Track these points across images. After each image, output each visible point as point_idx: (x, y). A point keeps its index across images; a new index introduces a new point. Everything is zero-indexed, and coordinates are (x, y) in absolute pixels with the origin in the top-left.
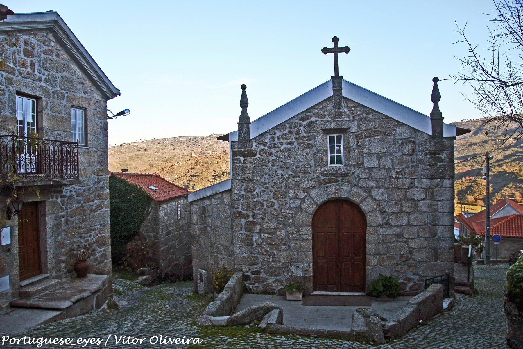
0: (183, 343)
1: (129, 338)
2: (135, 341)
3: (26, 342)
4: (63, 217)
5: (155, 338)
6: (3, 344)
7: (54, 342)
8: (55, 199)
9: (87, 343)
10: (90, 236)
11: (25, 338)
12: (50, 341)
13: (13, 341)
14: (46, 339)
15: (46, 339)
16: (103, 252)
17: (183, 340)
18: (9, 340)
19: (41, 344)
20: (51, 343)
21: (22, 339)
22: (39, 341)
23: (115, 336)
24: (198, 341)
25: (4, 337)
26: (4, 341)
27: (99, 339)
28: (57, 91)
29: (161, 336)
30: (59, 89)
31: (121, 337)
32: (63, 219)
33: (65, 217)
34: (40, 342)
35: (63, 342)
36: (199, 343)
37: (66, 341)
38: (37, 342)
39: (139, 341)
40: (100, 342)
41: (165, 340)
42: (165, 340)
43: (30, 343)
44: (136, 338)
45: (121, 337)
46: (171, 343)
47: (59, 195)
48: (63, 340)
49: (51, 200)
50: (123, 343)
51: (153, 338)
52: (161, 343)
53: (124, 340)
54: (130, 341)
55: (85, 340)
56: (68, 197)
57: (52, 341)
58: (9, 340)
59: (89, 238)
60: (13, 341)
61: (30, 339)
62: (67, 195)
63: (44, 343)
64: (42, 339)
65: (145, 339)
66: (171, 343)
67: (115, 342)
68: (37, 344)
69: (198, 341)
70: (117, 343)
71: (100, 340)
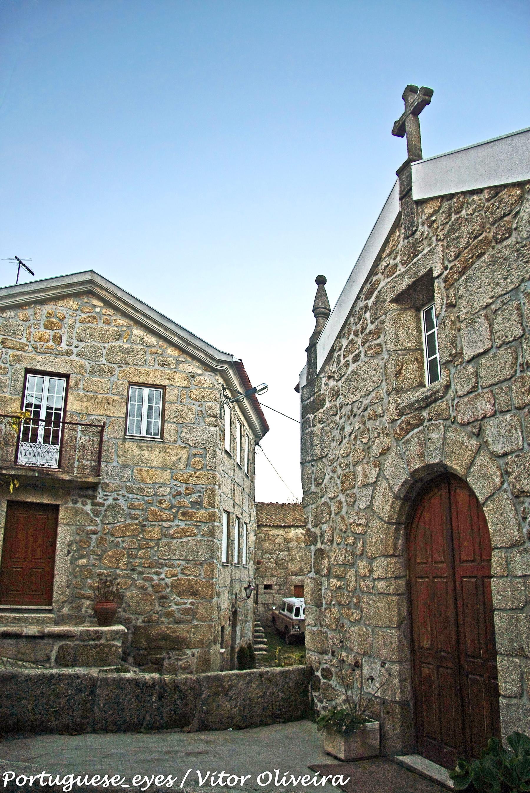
0: (315, 784)
1: (222, 775)
2: (232, 780)
3: (44, 782)
4: (95, 533)
5: (267, 776)
6: (5, 785)
7: (93, 781)
8: (79, 505)
9: (149, 784)
10: (158, 574)
11: (43, 774)
12: (86, 780)
13: (21, 780)
14: (79, 777)
15: (79, 777)
16: (188, 606)
17: (315, 779)
18: (15, 779)
19: (71, 785)
20: (87, 784)
21: (38, 776)
22: (66, 781)
23: (198, 772)
24: (341, 781)
25: (6, 774)
26: (6, 780)
27: (170, 776)
28: (99, 365)
29: (278, 771)
30: (104, 362)
31: (208, 773)
32: (94, 537)
33: (99, 534)
34: (70, 781)
35: (108, 782)
36: (342, 784)
37: (112, 780)
38: (63, 782)
39: (239, 781)
40: (171, 782)
41: (284, 779)
42: (284, 779)
43: (50, 784)
44: (234, 776)
45: (208, 773)
46: (295, 784)
47: (89, 502)
48: (109, 778)
49: (71, 505)
50: (212, 784)
51: (263, 775)
52: (276, 784)
53: (213, 778)
54: (224, 779)
55: (146, 778)
56: (108, 506)
57: (89, 779)
58: (15, 779)
59: (155, 577)
60: (21, 780)
61: (51, 778)
62: (107, 503)
63: (75, 784)
64: (72, 776)
65: (249, 776)
66: (295, 784)
67: (198, 782)
68: (63, 785)
69: (341, 781)
70: (201, 783)
71: (172, 779)
